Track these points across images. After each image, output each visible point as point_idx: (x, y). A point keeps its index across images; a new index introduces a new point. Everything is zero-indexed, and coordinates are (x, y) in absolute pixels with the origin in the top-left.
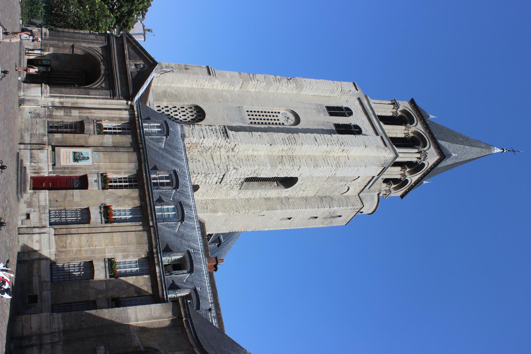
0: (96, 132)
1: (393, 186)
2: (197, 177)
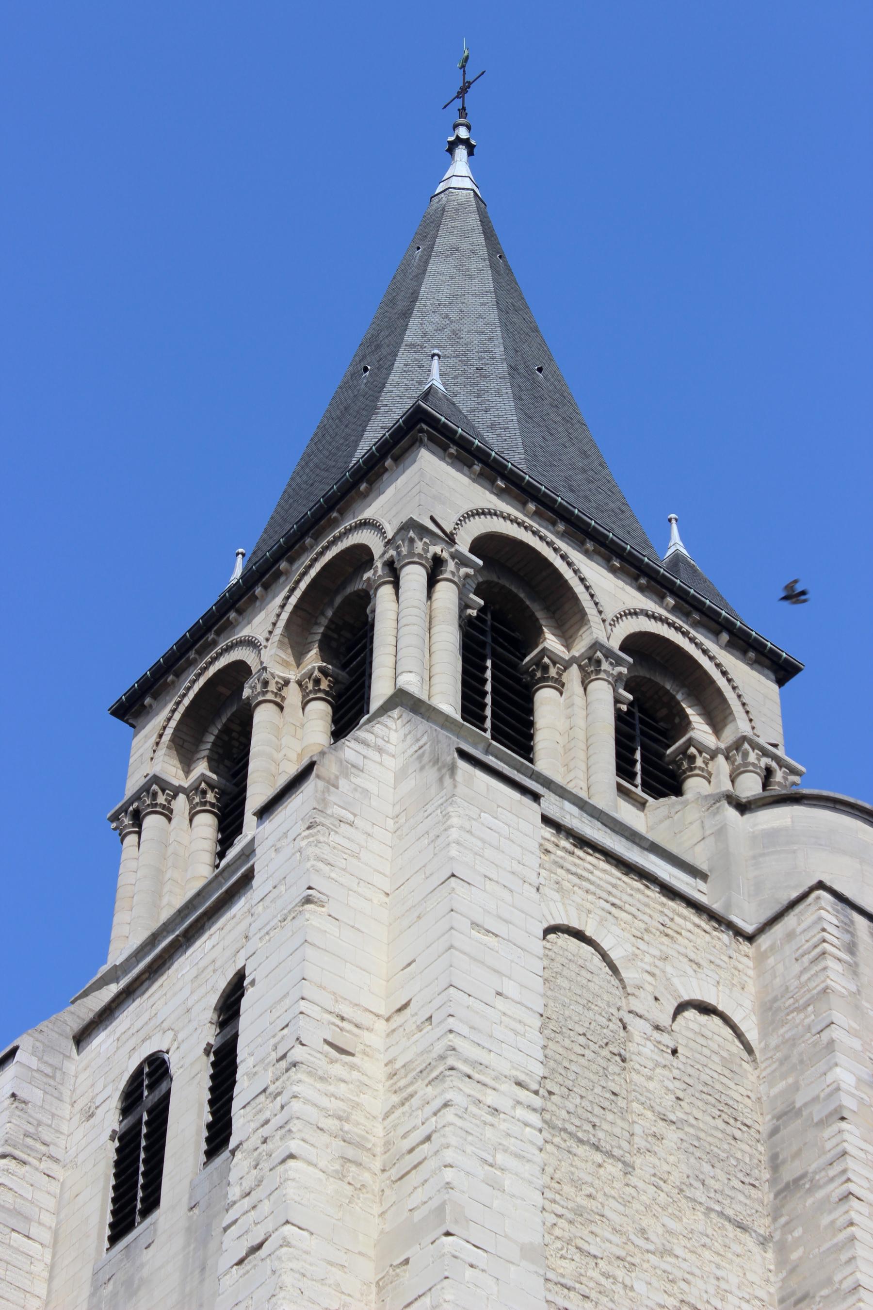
1: (700, 729)
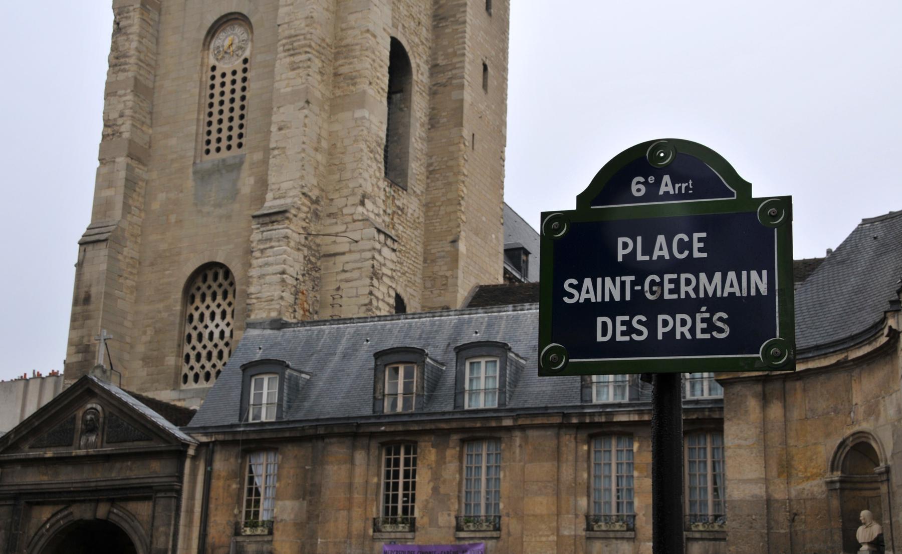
0: (269, 538)
2: (378, 299)
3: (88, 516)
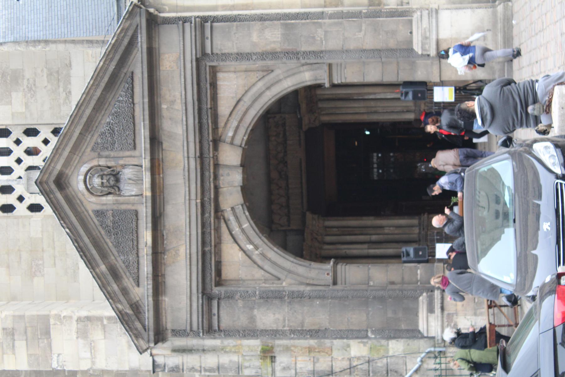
3: (237, 178)
